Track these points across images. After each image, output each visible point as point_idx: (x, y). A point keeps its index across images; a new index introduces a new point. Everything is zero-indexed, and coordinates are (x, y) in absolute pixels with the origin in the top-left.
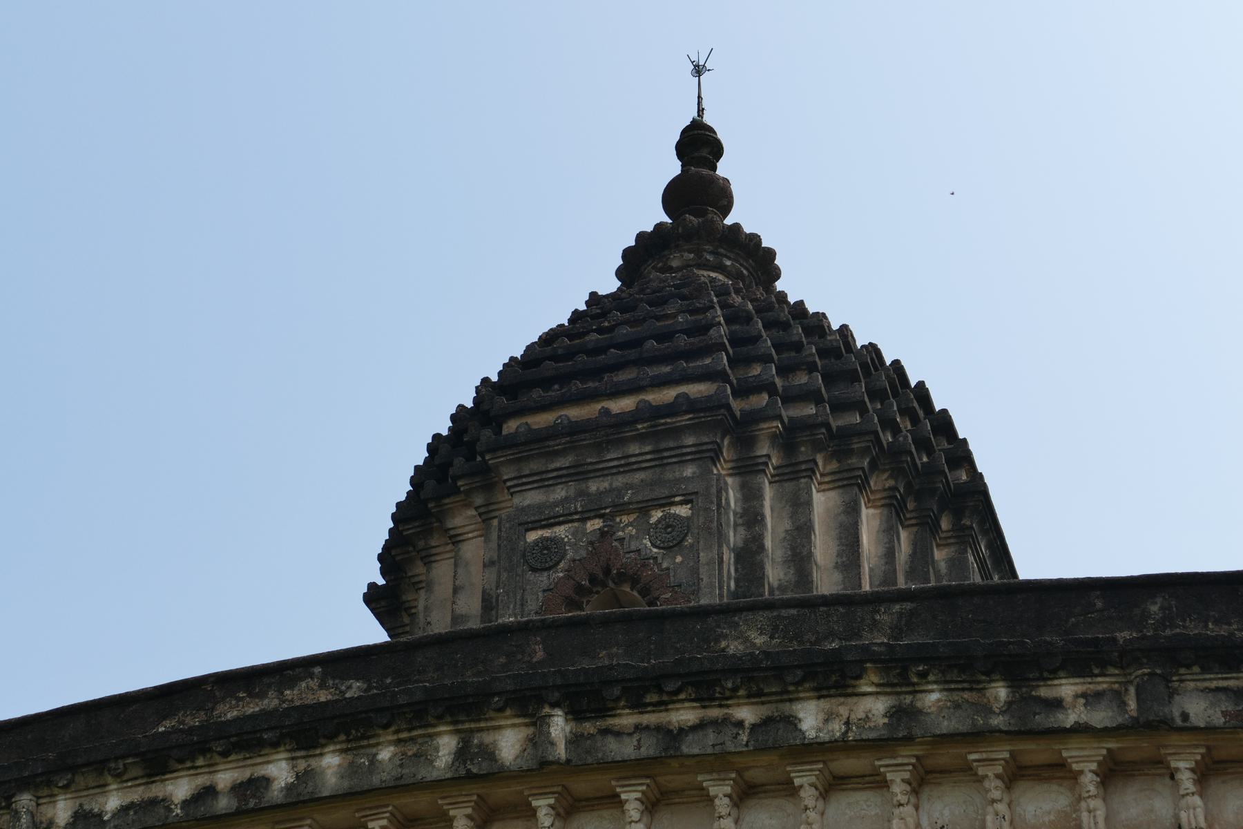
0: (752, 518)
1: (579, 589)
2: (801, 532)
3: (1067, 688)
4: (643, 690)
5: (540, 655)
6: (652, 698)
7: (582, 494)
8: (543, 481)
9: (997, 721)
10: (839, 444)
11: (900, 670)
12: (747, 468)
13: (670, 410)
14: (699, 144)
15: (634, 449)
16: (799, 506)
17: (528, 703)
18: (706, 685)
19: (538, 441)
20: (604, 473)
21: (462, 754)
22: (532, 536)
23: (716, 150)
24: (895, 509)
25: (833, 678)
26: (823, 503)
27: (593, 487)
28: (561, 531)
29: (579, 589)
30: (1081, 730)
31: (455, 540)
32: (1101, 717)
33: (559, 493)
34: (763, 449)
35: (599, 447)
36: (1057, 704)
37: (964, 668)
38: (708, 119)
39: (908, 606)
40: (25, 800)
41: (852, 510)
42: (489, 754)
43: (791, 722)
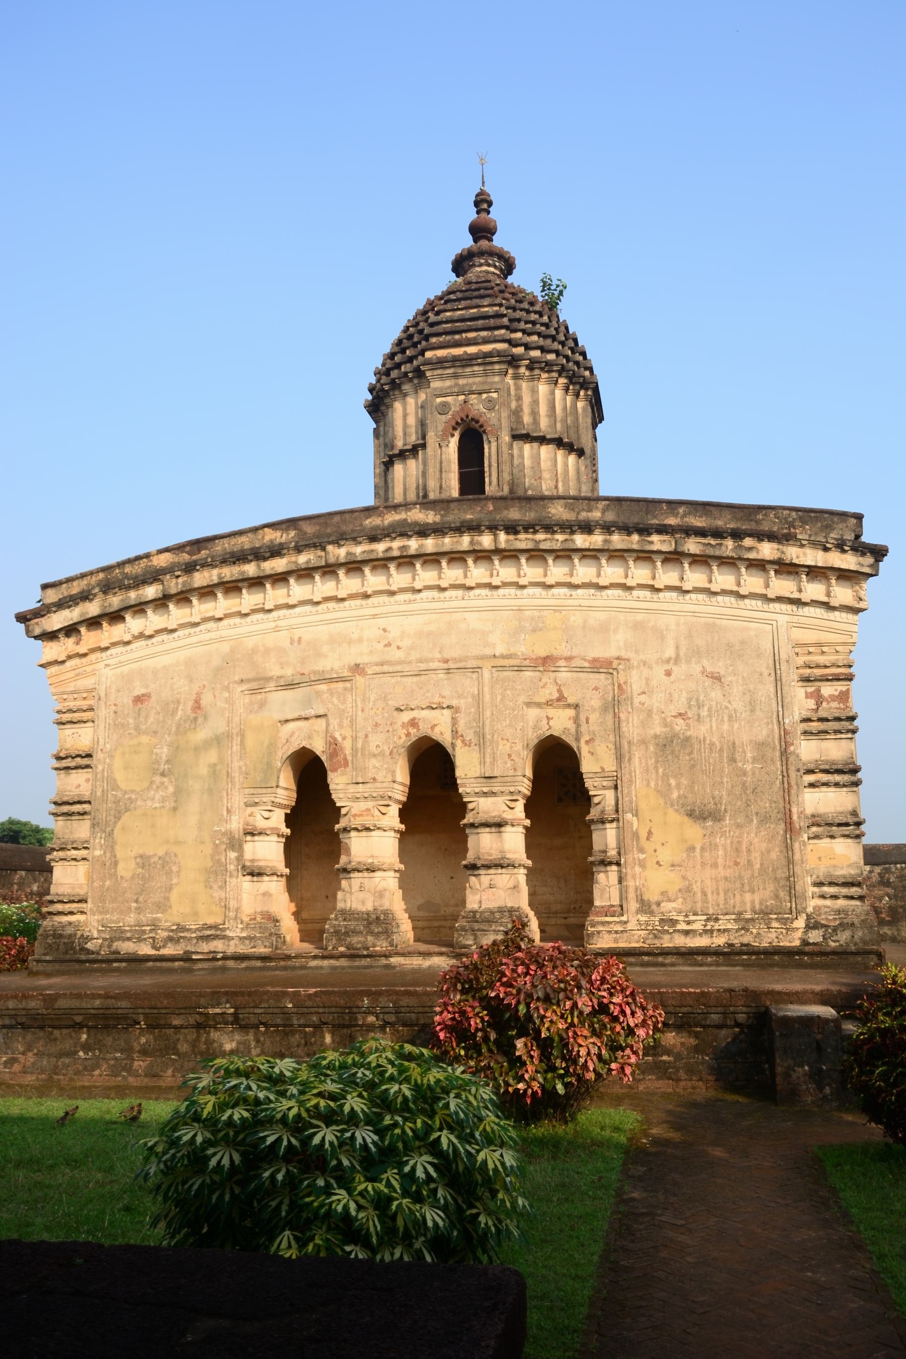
0: (519, 398)
1: (457, 423)
2: (535, 402)
3: (655, 538)
4: (530, 527)
5: (491, 508)
6: (531, 530)
7: (457, 385)
8: (441, 378)
9: (635, 547)
10: (548, 367)
11: (608, 528)
12: (516, 377)
13: (489, 355)
14: (482, 202)
15: (476, 368)
16: (534, 391)
17: (493, 528)
18: (549, 528)
19: (441, 363)
20: (464, 377)
21: (472, 543)
22: (439, 400)
23: (490, 204)
24: (567, 390)
25: (587, 528)
26: (543, 389)
27: (461, 382)
28: (449, 399)
29: (457, 423)
30: (659, 552)
31: (405, 395)
32: (665, 548)
33: (448, 383)
34: (523, 370)
35: (463, 366)
36: (652, 543)
37: (627, 530)
38: (487, 189)
39: (607, 502)
40: (330, 548)
41: (553, 393)
42: (480, 544)
43: (573, 541)
